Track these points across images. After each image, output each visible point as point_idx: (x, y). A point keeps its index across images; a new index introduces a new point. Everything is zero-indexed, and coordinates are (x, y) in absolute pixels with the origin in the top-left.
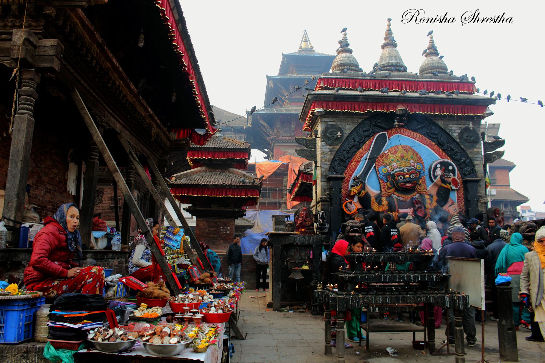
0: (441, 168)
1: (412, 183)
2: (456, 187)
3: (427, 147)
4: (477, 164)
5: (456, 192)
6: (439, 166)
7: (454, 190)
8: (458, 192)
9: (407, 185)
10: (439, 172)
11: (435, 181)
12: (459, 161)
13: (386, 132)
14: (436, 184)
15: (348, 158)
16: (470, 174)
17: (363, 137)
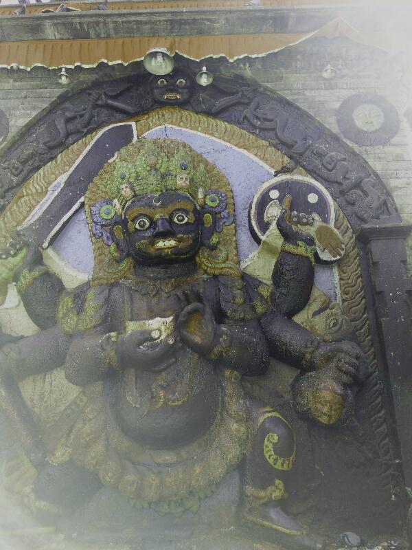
0: (281, 199)
1: (179, 241)
2: (334, 251)
3: (245, 152)
4: (397, 187)
5: (335, 271)
6: (274, 194)
7: (328, 264)
8: (341, 271)
9: (161, 244)
10: (273, 211)
11: (263, 238)
12: (340, 184)
13: (133, 124)
14: (270, 249)
15: (11, 188)
16: (378, 218)
17: (63, 132)
